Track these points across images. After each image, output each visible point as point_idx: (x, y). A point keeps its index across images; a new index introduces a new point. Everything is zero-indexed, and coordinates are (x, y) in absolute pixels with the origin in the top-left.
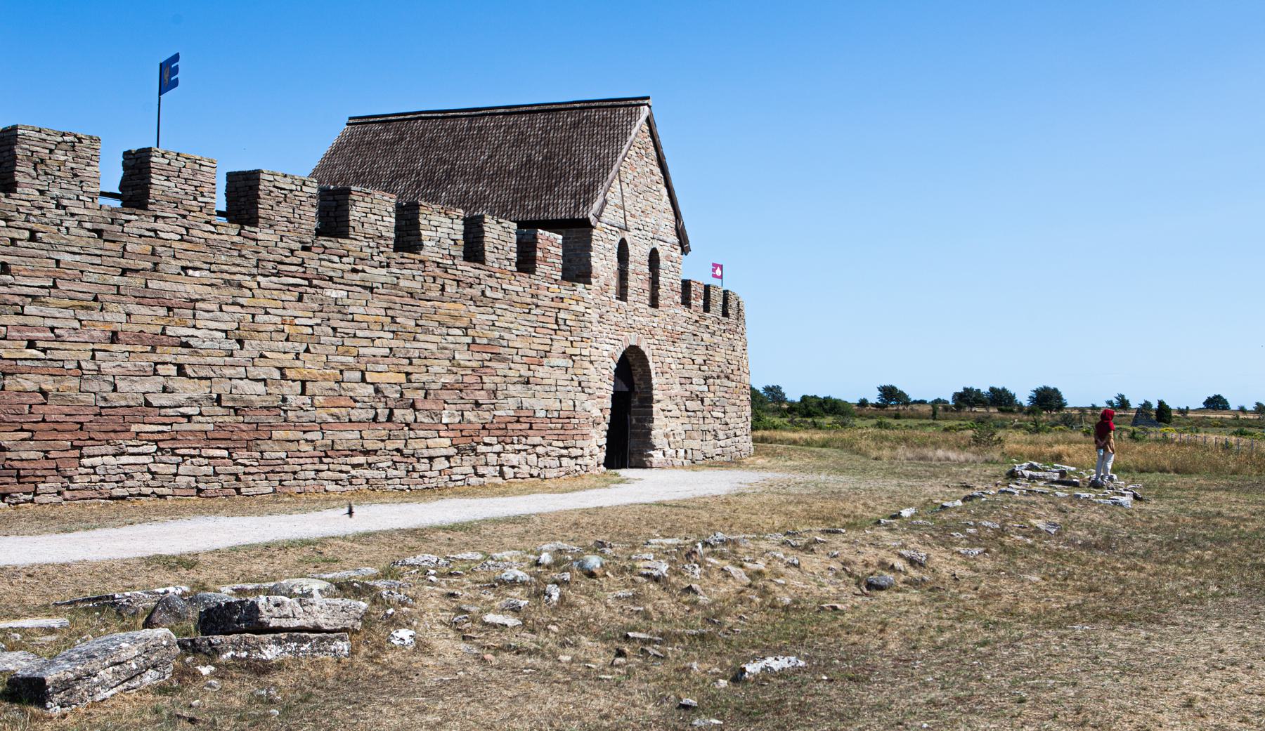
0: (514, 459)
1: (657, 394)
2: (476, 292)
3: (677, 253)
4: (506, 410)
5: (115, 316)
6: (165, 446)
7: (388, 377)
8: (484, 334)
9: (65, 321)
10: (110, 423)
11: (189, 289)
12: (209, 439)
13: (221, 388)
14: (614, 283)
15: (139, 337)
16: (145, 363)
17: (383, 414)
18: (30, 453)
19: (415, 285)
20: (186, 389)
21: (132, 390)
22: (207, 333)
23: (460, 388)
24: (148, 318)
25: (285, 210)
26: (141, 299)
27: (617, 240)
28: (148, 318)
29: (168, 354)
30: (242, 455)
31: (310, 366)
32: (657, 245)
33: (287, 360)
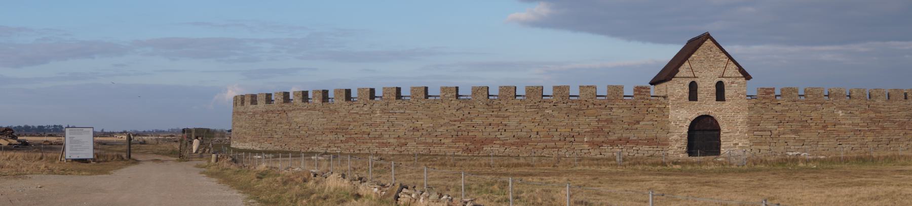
4: (613, 137)
5: (490, 120)
7: (562, 130)
9: (480, 122)
11: (508, 114)
12: (513, 145)
13: (515, 134)
14: (687, 96)
16: (496, 129)
17: (562, 138)
18: (472, 147)
19: (578, 107)
20: (505, 135)
22: (513, 123)
23: (593, 132)
24: (497, 121)
26: (497, 116)
27: (688, 82)
28: (497, 121)
29: (501, 127)
31: (539, 128)
32: (723, 80)
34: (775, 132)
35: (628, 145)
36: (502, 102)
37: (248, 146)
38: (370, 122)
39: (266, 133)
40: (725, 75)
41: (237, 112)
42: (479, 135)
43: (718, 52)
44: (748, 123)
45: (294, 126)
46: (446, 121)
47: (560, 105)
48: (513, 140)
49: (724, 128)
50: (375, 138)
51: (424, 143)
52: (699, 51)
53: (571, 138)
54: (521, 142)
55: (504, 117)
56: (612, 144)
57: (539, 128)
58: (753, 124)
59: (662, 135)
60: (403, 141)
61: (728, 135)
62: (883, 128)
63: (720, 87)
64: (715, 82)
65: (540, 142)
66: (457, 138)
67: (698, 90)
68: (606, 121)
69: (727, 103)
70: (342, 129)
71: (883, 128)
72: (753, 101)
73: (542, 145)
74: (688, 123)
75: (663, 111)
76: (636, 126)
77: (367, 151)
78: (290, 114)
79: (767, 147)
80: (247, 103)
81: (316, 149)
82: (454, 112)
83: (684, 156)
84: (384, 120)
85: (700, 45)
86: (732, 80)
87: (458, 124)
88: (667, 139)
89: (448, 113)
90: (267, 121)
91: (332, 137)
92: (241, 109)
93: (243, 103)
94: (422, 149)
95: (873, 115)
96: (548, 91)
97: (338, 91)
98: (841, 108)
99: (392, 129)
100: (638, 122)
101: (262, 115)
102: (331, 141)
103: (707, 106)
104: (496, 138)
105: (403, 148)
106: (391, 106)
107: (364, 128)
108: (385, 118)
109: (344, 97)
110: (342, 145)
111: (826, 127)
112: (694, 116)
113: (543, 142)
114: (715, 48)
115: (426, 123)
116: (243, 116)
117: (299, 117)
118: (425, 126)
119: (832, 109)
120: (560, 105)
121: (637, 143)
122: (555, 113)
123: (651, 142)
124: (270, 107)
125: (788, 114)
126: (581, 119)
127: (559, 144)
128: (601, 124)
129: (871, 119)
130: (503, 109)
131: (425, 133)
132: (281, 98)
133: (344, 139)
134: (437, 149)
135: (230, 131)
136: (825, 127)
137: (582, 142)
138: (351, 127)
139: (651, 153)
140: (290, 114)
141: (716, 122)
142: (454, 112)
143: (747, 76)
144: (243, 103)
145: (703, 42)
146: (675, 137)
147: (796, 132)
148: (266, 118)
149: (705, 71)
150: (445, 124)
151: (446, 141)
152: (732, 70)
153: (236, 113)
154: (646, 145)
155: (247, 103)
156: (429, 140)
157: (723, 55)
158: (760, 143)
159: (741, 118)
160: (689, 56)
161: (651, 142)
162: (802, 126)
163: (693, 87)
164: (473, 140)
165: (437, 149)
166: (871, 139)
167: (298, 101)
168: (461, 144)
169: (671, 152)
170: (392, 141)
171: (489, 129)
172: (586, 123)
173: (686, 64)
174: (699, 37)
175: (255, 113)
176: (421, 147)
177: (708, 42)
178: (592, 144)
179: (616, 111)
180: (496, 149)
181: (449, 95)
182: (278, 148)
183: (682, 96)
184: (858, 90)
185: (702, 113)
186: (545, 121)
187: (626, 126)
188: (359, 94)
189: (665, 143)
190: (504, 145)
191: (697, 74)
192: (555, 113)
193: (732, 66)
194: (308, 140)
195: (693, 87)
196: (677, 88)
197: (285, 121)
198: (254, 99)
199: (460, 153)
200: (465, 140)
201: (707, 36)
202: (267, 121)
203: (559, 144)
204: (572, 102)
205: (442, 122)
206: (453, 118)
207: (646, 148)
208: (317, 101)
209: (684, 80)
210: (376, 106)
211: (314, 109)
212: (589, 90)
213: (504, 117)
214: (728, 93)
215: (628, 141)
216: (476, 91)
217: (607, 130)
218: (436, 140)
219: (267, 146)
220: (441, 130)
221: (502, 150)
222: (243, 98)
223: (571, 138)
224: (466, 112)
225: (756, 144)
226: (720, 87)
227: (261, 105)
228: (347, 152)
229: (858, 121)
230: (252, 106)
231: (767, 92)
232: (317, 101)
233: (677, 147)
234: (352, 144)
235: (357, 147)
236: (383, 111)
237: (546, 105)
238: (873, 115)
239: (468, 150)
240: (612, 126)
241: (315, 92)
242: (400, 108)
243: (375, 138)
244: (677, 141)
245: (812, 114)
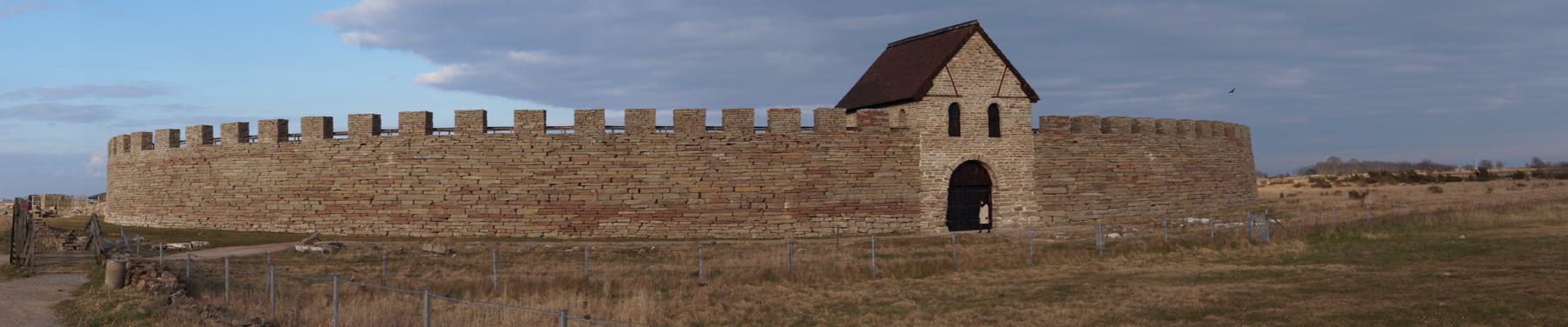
0: (843, 224)
1: (1003, 185)
2: (813, 145)
3: (1025, 103)
4: (836, 200)
5: (612, 172)
8: (815, 165)
9: (592, 175)
11: (645, 160)
12: (654, 217)
13: (659, 197)
15: (622, 180)
16: (624, 189)
19: (770, 147)
20: (639, 199)
21: (617, 200)
22: (653, 177)
24: (624, 172)
25: (689, 123)
26: (624, 165)
27: (947, 103)
28: (624, 172)
29: (631, 185)
30: (669, 223)
31: (703, 186)
32: (999, 101)
33: (690, 185)
34: (1073, 188)
35: (858, 214)
36: (632, 139)
37: (138, 221)
38: (373, 177)
39: (171, 198)
40: (1002, 93)
41: (118, 164)
42: (591, 201)
43: (991, 55)
44: (1034, 174)
45: (223, 184)
46: (526, 173)
47: (739, 144)
48: (652, 210)
49: (1000, 181)
50: (384, 207)
51: (483, 216)
52: (963, 52)
53: (758, 205)
54: (671, 212)
55: (637, 167)
56: (832, 212)
57: (703, 186)
58: (1042, 175)
59: (909, 195)
60: (442, 212)
61: (1006, 194)
62: (1197, 180)
63: (994, 111)
64: (987, 104)
65: (705, 211)
66: (549, 205)
67: (962, 118)
68: (820, 171)
69: (1005, 140)
70: (319, 190)
71: (1197, 180)
72: (1040, 137)
73: (711, 216)
74: (949, 173)
75: (911, 154)
76: (869, 180)
77: (368, 231)
78: (215, 165)
79: (1062, 213)
80: (136, 148)
81: (267, 227)
82: (542, 156)
83: (942, 231)
84: (402, 173)
85: (964, 42)
86: (1012, 101)
87: (550, 180)
88: (917, 202)
89: (530, 158)
90: (173, 177)
91: (297, 204)
92: (123, 157)
93: (127, 148)
94: (479, 227)
95: (1185, 160)
96: (714, 118)
97: (308, 122)
98: (1152, 149)
99: (419, 189)
100: (871, 173)
101: (163, 168)
102: (297, 213)
103: (976, 145)
105: (441, 226)
106: (415, 147)
107: (362, 189)
108: (404, 168)
109: (321, 131)
110: (318, 220)
111: (1135, 178)
112: (957, 162)
113: (712, 211)
114: (986, 48)
115: (486, 179)
116: (128, 170)
117: (235, 170)
118: (484, 183)
120: (739, 144)
121: (870, 209)
122: (731, 159)
123: (895, 207)
124: (174, 153)
125: (1088, 160)
126: (778, 170)
127: (739, 215)
128: (811, 178)
130: (635, 152)
131: (484, 196)
132: (198, 137)
133: (321, 208)
134: (509, 227)
135: (102, 197)
136: (1135, 178)
137: (781, 210)
138: (336, 186)
139: (894, 226)
140: (215, 165)
141: (986, 172)
142: (542, 156)
143: (1032, 96)
144: (127, 148)
145: (969, 36)
146: (930, 198)
147: (1099, 187)
148: (170, 171)
149: (968, 82)
150: (523, 181)
151: (527, 211)
152: (1011, 86)
153: (114, 167)
154: (886, 212)
155: (136, 148)
156: (494, 210)
157: (999, 60)
159: (1024, 165)
160: (949, 59)
161: (895, 207)
162: (1109, 178)
163: (954, 111)
164: (580, 210)
165: (509, 227)
166: (1185, 195)
167: (232, 141)
168: (557, 218)
169: (924, 224)
170: (418, 211)
171: (610, 189)
172: (785, 174)
173: (944, 73)
174: (961, 27)
175: (149, 165)
176: (478, 223)
177: (977, 37)
178: (803, 215)
179: (835, 155)
180: (622, 227)
181: (532, 125)
182: (194, 224)
183: (939, 128)
184: (1168, 121)
185: (968, 156)
186: (712, 173)
187: (852, 180)
188: (351, 125)
189: (913, 209)
190: (638, 217)
191: (960, 91)
192: (731, 159)
193: (1011, 79)
194: (251, 210)
195: (954, 111)
196: (928, 115)
197: (206, 177)
198: (147, 141)
199: (554, 234)
200: (564, 209)
201: (975, 27)
202: (173, 177)
203: (739, 215)
204: (760, 137)
205: (518, 175)
206: (540, 169)
207: (886, 218)
208: (267, 140)
209: (938, 101)
210: (386, 146)
211: (262, 154)
212: (789, 117)
213: (637, 167)
214: (1006, 123)
215: (857, 206)
217: (821, 187)
218: (506, 209)
219: (172, 221)
220: (516, 190)
221: (634, 227)
222: (127, 140)
223: (758, 205)
224: (565, 157)
225: (1047, 208)
226: (994, 111)
227: (162, 150)
228: (329, 232)
229: (1171, 168)
230: (143, 153)
231: (1060, 121)
232: (267, 140)
233: (932, 220)
234: (338, 217)
235: (349, 223)
236: (400, 156)
237: (712, 144)
239: (570, 228)
240: (830, 181)
241: (263, 124)
242: (433, 150)
243: (384, 207)
244: (933, 205)
245: (1120, 159)
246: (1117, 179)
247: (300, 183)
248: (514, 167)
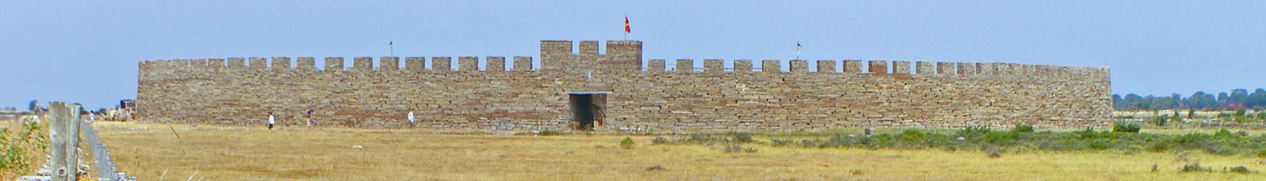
5: (372, 92)
6: (383, 118)
8: (481, 90)
10: (369, 114)
20: (385, 106)
22: (393, 95)
62: (803, 105)
71: (803, 105)
91: (225, 109)
95: (788, 90)
100: (516, 95)
104: (377, 111)
107: (254, 100)
111: (723, 103)
119: (733, 83)
122: (434, 85)
127: (438, 117)
129: (786, 94)
136: (723, 103)
151: (330, 113)
158: (647, 120)
171: (370, 102)
205: (327, 93)
215: (506, 114)
216: (358, 61)
236: (272, 83)
238: (788, 90)
246: (705, 103)
247: (227, 97)
248: (324, 89)
